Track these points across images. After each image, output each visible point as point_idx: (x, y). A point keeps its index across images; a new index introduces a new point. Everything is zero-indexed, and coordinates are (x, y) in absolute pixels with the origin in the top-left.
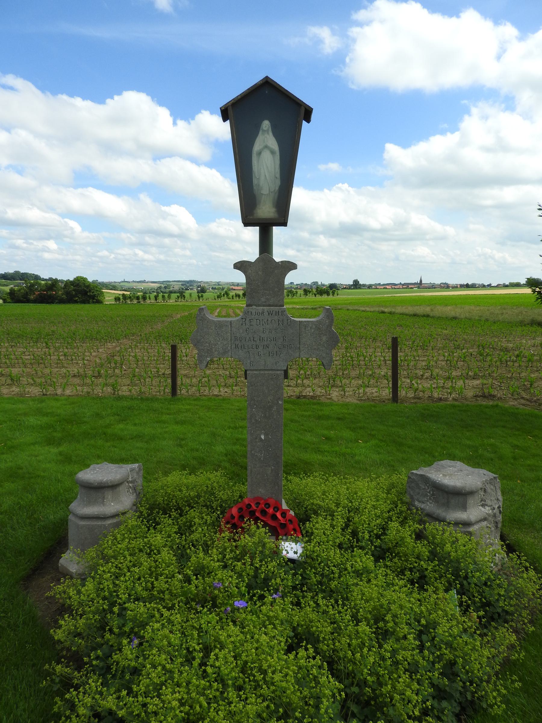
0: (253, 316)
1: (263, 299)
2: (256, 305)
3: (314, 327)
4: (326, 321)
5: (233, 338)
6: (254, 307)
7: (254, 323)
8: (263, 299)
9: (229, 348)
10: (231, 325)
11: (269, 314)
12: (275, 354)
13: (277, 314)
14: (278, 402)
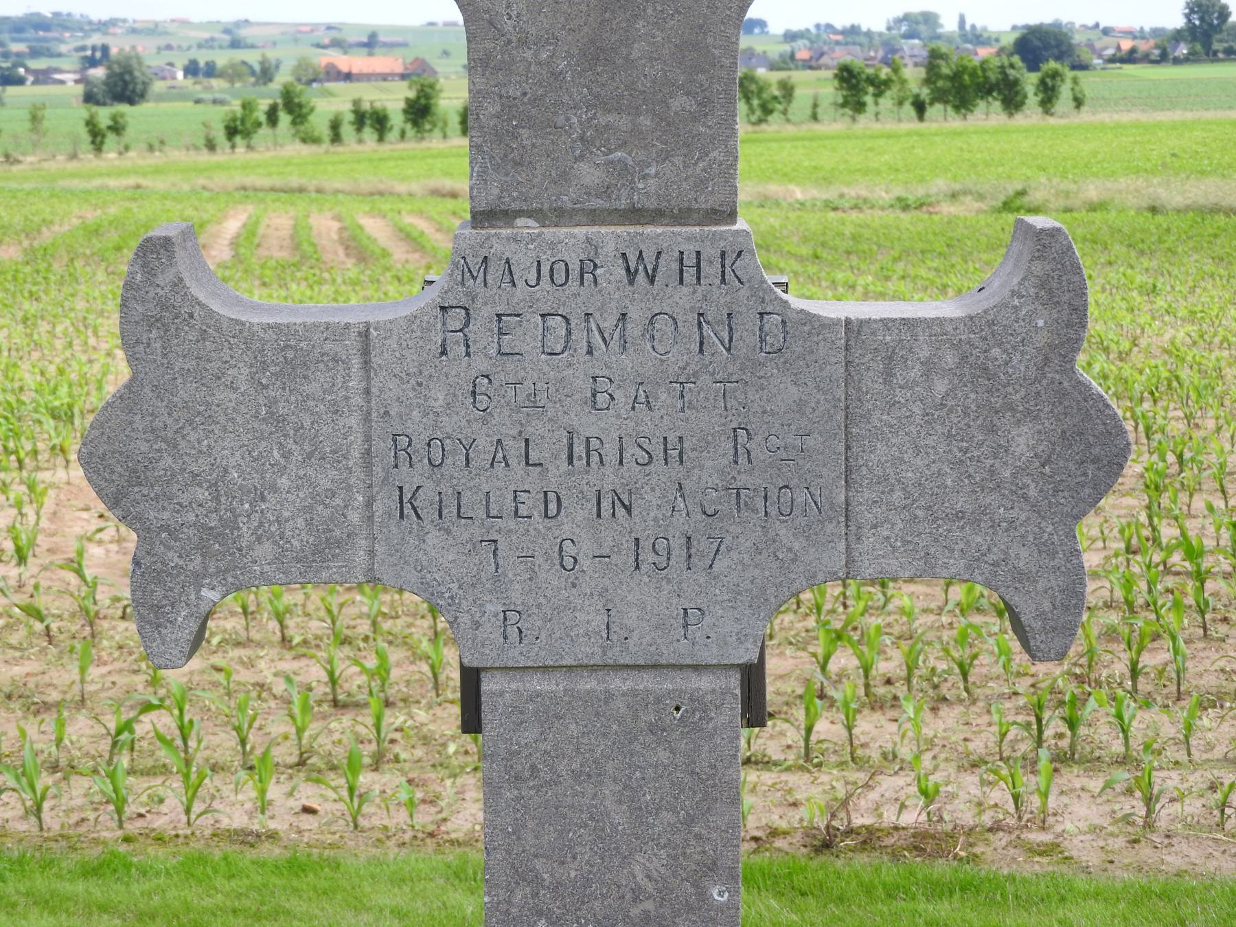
0: (521, 291)
1: (589, 174)
2: (537, 215)
3: (950, 359)
4: (1031, 315)
5: (382, 446)
6: (526, 226)
7: (526, 337)
8: (589, 174)
9: (355, 517)
10: (366, 352)
11: (631, 275)
12: (679, 553)
14: (703, 896)
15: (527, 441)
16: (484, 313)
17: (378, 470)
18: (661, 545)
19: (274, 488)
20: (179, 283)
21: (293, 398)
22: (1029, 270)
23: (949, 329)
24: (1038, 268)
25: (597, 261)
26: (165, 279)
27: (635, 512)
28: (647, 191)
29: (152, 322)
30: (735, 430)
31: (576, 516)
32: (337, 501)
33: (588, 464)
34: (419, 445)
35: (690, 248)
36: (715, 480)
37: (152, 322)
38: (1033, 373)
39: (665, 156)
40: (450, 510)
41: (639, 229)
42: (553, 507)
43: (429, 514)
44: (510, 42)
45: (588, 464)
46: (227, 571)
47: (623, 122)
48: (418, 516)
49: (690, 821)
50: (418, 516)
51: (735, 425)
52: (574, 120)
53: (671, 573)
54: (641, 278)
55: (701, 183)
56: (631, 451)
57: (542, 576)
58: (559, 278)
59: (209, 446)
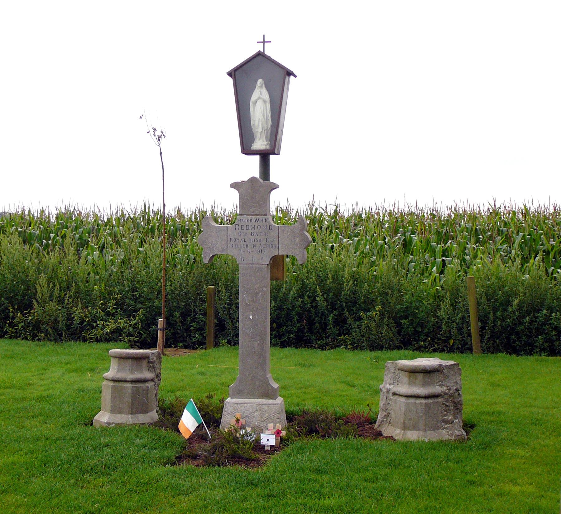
3: (290, 230)
5: (229, 239)
6: (245, 216)
7: (244, 228)
8: (251, 210)
28: (257, 212)
47: (255, 205)
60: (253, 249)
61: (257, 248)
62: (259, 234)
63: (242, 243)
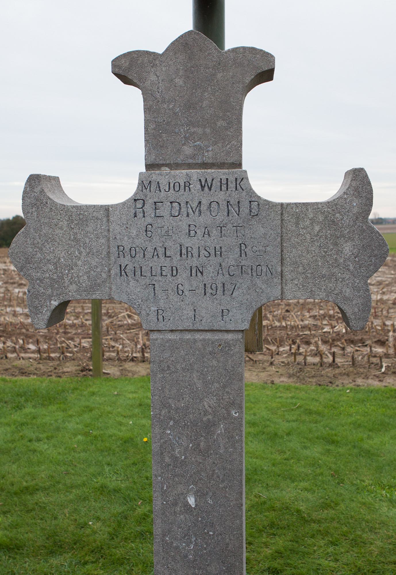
0: (163, 193)
1: (188, 150)
3: (321, 218)
4: (351, 201)
5: (114, 250)
6: (166, 170)
7: (164, 210)
8: (188, 150)
9: (104, 275)
11: (203, 187)
13: (224, 187)
14: (229, 413)
15: (165, 248)
16: (150, 202)
17: (112, 258)
18: (214, 286)
19: (76, 265)
20: (42, 191)
21: (82, 233)
22: (350, 185)
23: (320, 206)
24: (354, 184)
25: (190, 182)
26: (37, 190)
27: (204, 274)
28: (208, 156)
29: (33, 205)
30: (240, 244)
31: (183, 277)
32: (99, 270)
33: (187, 257)
34: (127, 249)
35: (224, 177)
36: (233, 263)
37: (33, 205)
38: (352, 223)
39: (215, 143)
40: (138, 273)
41: (206, 170)
42: (175, 272)
43: (131, 274)
44: (158, 101)
45: (187, 257)
46: (60, 294)
47: (200, 131)
48: (127, 275)
49: (224, 387)
50: (127, 275)
51: (240, 242)
52: (182, 130)
53: (217, 296)
54: (206, 188)
55: (228, 153)
56: (203, 252)
57: (171, 297)
58: (177, 189)
59: (53, 250)
60: (197, 282)
61: (207, 278)
62: (215, 232)
63: (156, 264)
